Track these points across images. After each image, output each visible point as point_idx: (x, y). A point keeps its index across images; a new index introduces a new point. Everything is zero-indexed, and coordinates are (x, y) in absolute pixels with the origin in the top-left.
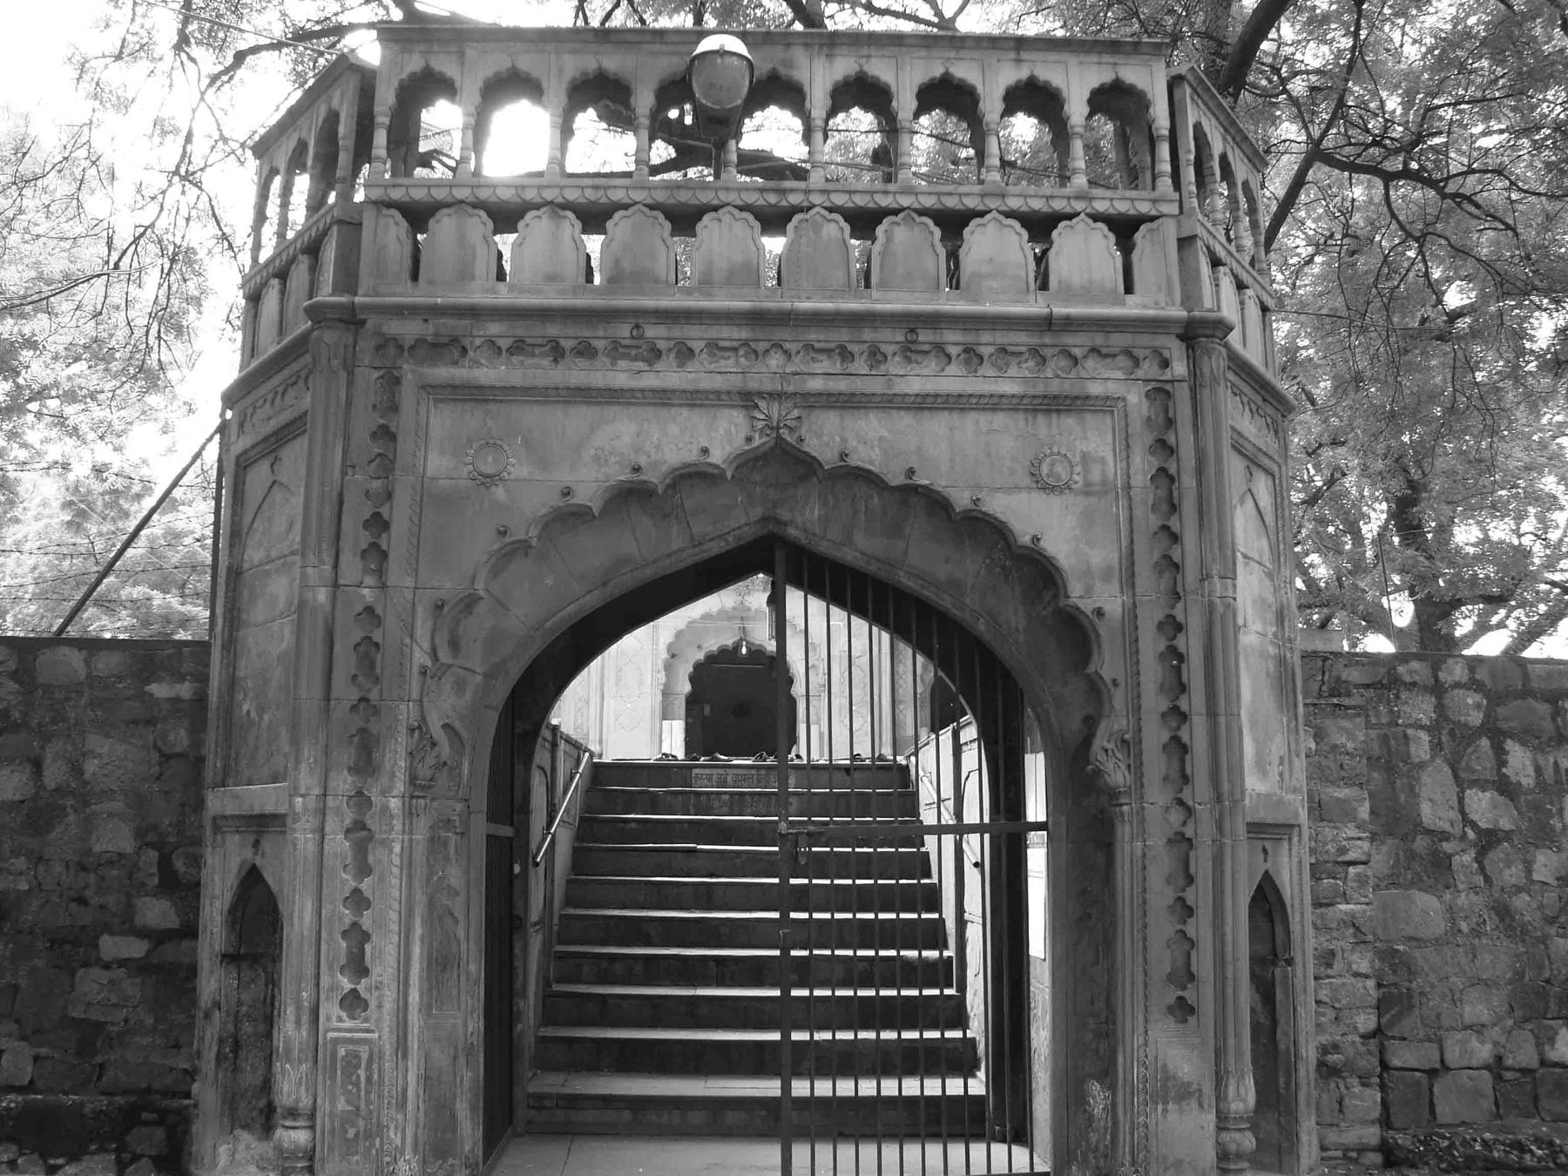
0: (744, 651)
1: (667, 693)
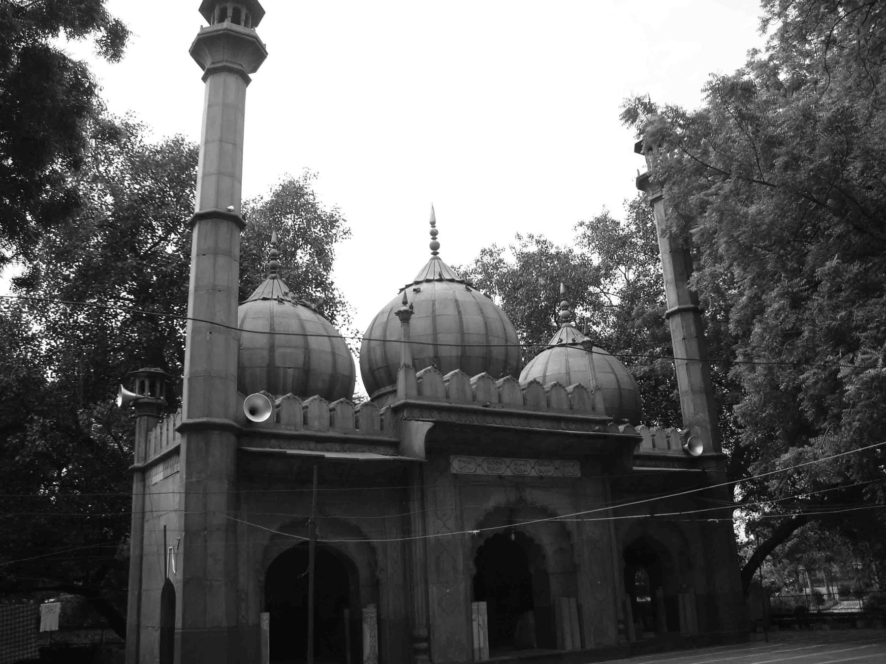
0: (513, 537)
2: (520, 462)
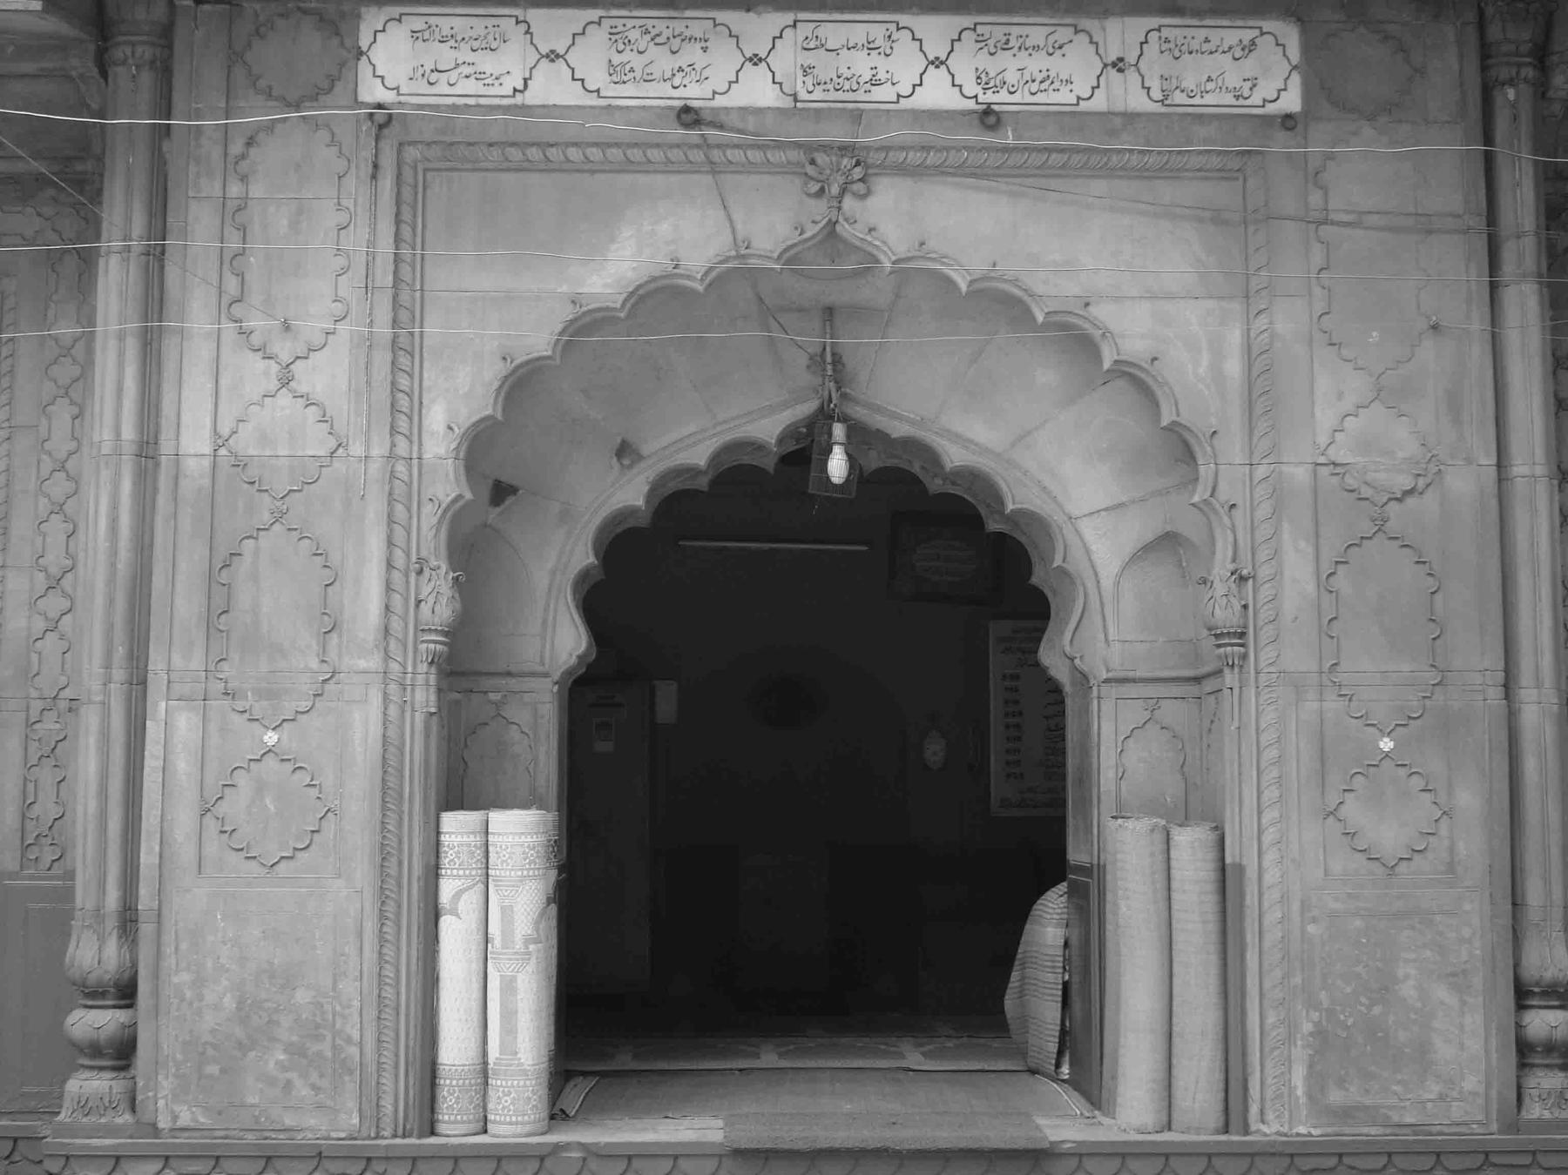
0: (837, 466)
1: (464, 667)
2: (840, 31)
